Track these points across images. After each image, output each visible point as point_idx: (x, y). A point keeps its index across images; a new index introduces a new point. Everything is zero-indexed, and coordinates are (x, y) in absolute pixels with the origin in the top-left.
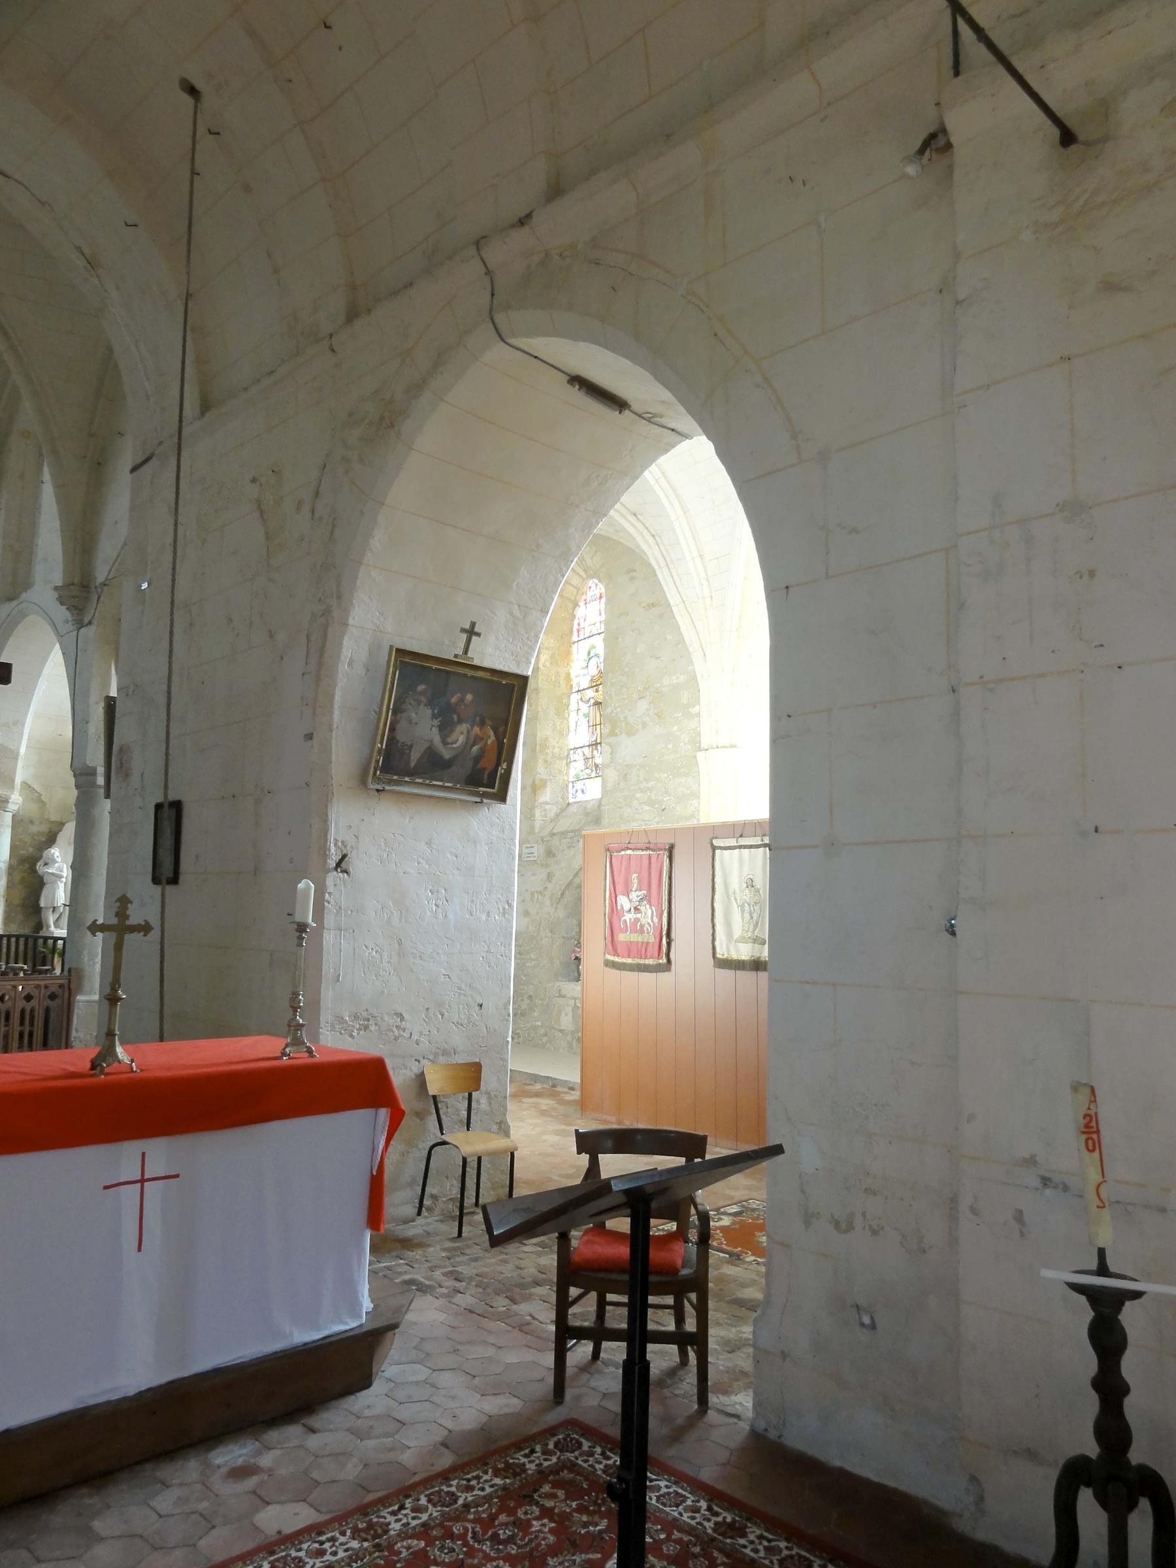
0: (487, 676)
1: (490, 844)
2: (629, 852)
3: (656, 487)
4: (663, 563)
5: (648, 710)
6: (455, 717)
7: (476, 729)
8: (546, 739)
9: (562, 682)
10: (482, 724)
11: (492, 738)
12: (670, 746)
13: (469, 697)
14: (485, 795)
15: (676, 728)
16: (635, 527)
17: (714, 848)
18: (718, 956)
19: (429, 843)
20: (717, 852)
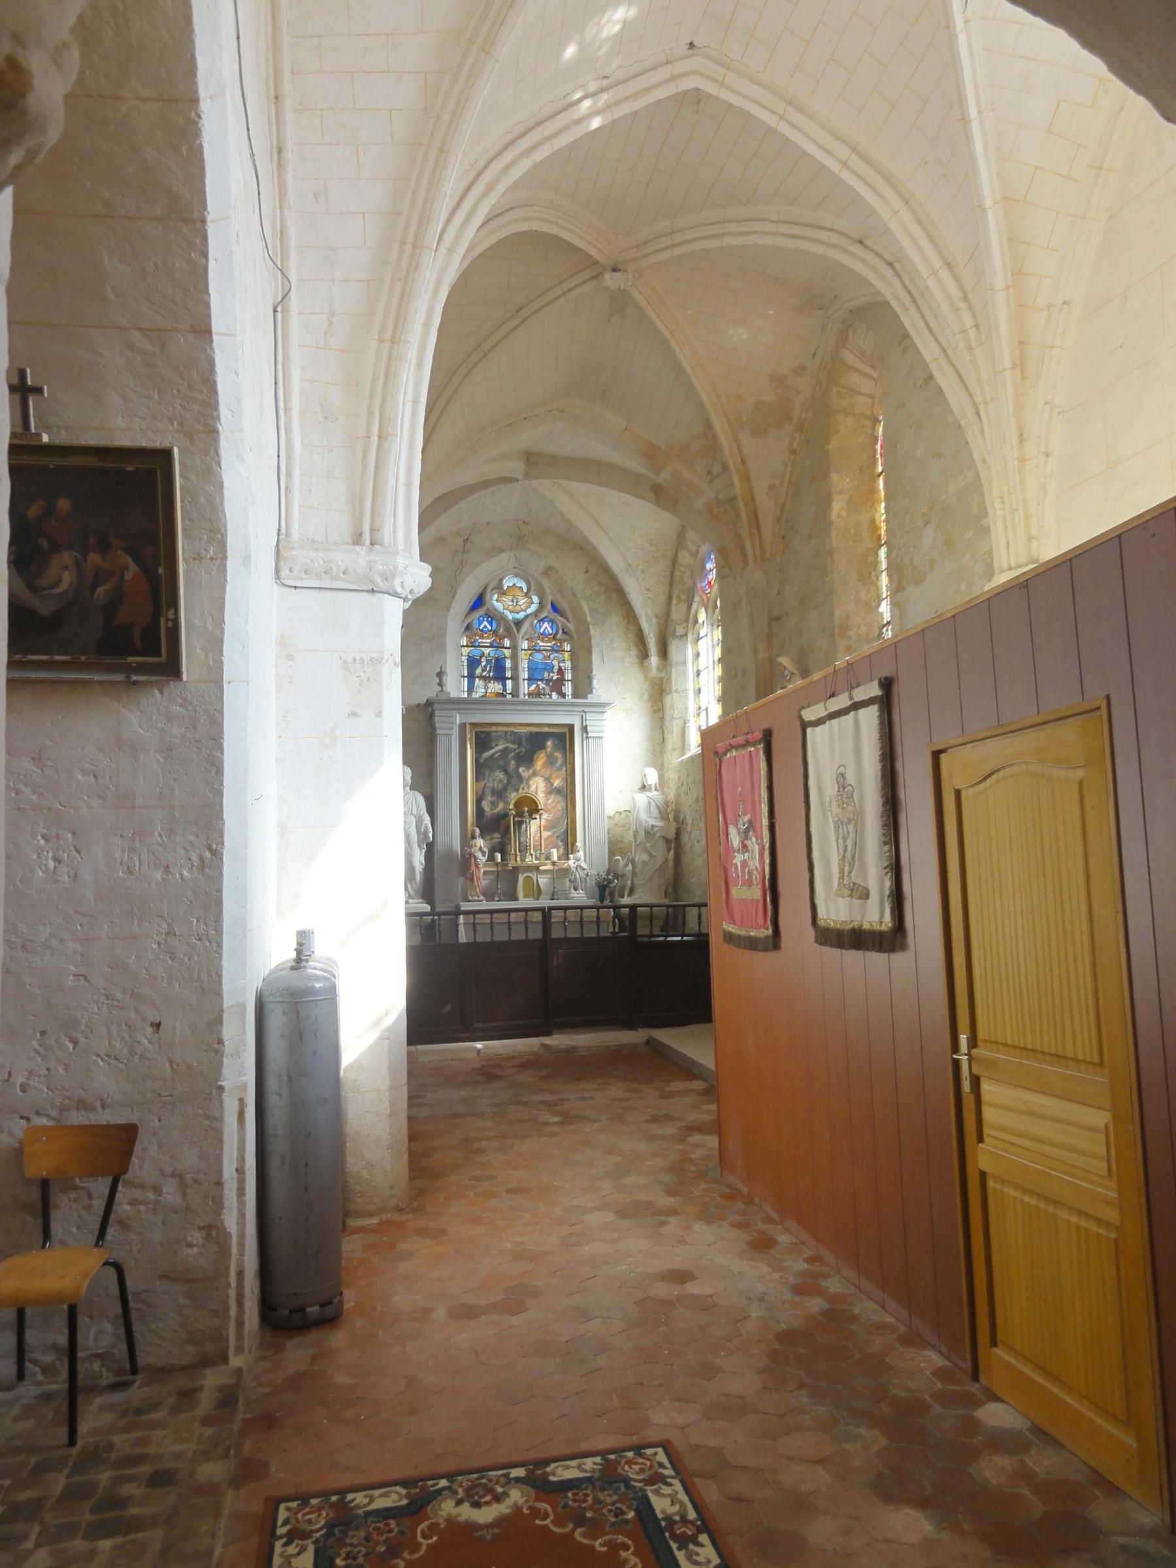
0: (91, 461)
1: (168, 750)
2: (734, 753)
3: (846, 176)
4: (907, 300)
5: (934, 539)
6: (45, 545)
7: (94, 558)
8: (848, 617)
9: (866, 534)
10: (104, 547)
11: (132, 570)
12: (963, 587)
13: (63, 504)
14: (142, 669)
15: (968, 556)
16: (863, 261)
17: (804, 725)
18: (821, 923)
19: (37, 759)
20: (809, 730)
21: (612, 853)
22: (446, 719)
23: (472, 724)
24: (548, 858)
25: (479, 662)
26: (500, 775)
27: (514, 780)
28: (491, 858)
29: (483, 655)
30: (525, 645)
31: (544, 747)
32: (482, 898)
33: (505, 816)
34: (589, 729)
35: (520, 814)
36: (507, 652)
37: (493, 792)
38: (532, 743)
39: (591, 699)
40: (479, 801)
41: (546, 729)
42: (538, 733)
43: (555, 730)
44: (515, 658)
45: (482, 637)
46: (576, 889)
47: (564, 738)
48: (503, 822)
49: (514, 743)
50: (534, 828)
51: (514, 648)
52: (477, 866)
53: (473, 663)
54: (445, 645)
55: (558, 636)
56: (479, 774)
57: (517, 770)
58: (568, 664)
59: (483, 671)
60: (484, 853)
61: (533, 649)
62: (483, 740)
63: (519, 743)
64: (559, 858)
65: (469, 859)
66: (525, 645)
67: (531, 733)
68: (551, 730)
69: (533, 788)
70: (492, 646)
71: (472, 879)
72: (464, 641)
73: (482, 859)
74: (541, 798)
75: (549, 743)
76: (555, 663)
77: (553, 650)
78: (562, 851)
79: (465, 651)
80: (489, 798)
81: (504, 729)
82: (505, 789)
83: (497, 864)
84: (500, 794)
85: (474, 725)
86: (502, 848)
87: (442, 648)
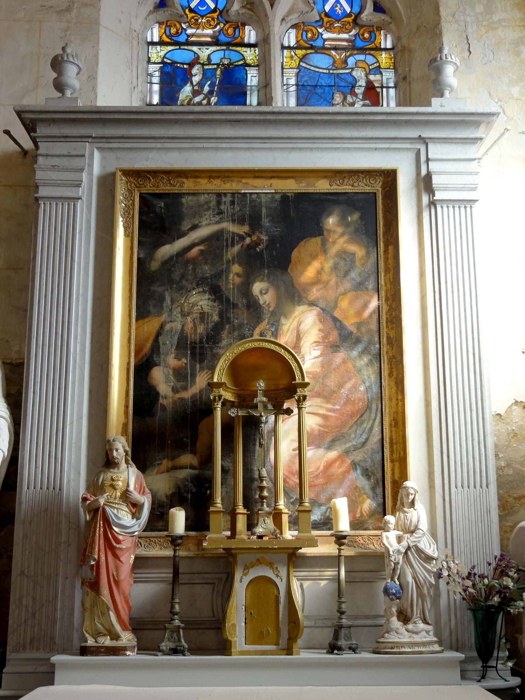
21: (507, 508)
22: (65, 162)
23: (127, 173)
24: (327, 523)
25: (187, 77)
26: (201, 301)
27: (237, 311)
28: (159, 519)
29: (196, 61)
30: (291, 38)
31: (318, 231)
32: (127, 638)
33: (203, 409)
34: (436, 180)
35: (245, 400)
36: (250, 55)
37: (183, 344)
38: (286, 223)
39: (437, 105)
40: (142, 370)
41: (323, 186)
42: (300, 197)
43: (346, 188)
44: (264, 65)
45: (197, 25)
46: (404, 617)
47: (372, 207)
48: (203, 425)
49: (241, 221)
50: (287, 439)
51: (263, 43)
52: (111, 546)
53: (173, 77)
54: (96, 23)
55: (364, 16)
56: (146, 300)
57: (245, 289)
58: (389, 77)
59: (196, 93)
60: (135, 508)
61: (309, 46)
62: (159, 213)
63: (254, 222)
64: (355, 524)
65: (91, 525)
66: (291, 38)
67: (285, 198)
68: (336, 188)
69: (285, 338)
70: (216, 42)
71: (94, 586)
72: (155, 34)
73: (127, 522)
74: (310, 359)
75: (331, 221)
76: (359, 74)
77: (353, 48)
78: (368, 505)
79: (157, 53)
80: (172, 361)
81: (217, 185)
82: (213, 337)
83: (175, 541)
84: (200, 351)
85: (135, 175)
86: (196, 498)
87: (90, 29)
